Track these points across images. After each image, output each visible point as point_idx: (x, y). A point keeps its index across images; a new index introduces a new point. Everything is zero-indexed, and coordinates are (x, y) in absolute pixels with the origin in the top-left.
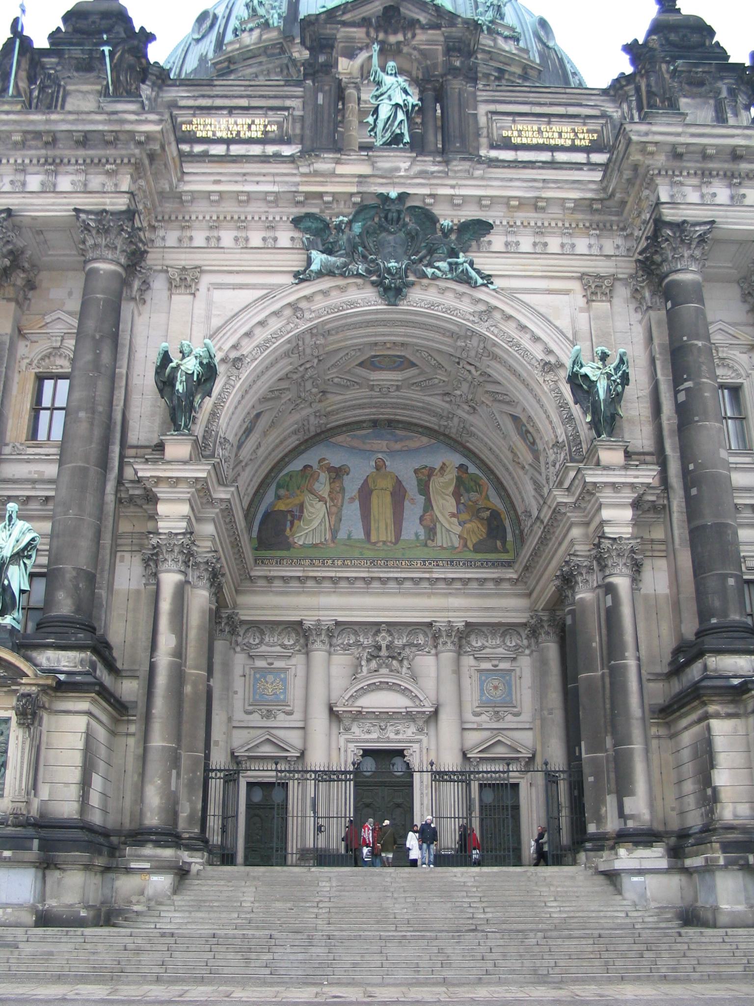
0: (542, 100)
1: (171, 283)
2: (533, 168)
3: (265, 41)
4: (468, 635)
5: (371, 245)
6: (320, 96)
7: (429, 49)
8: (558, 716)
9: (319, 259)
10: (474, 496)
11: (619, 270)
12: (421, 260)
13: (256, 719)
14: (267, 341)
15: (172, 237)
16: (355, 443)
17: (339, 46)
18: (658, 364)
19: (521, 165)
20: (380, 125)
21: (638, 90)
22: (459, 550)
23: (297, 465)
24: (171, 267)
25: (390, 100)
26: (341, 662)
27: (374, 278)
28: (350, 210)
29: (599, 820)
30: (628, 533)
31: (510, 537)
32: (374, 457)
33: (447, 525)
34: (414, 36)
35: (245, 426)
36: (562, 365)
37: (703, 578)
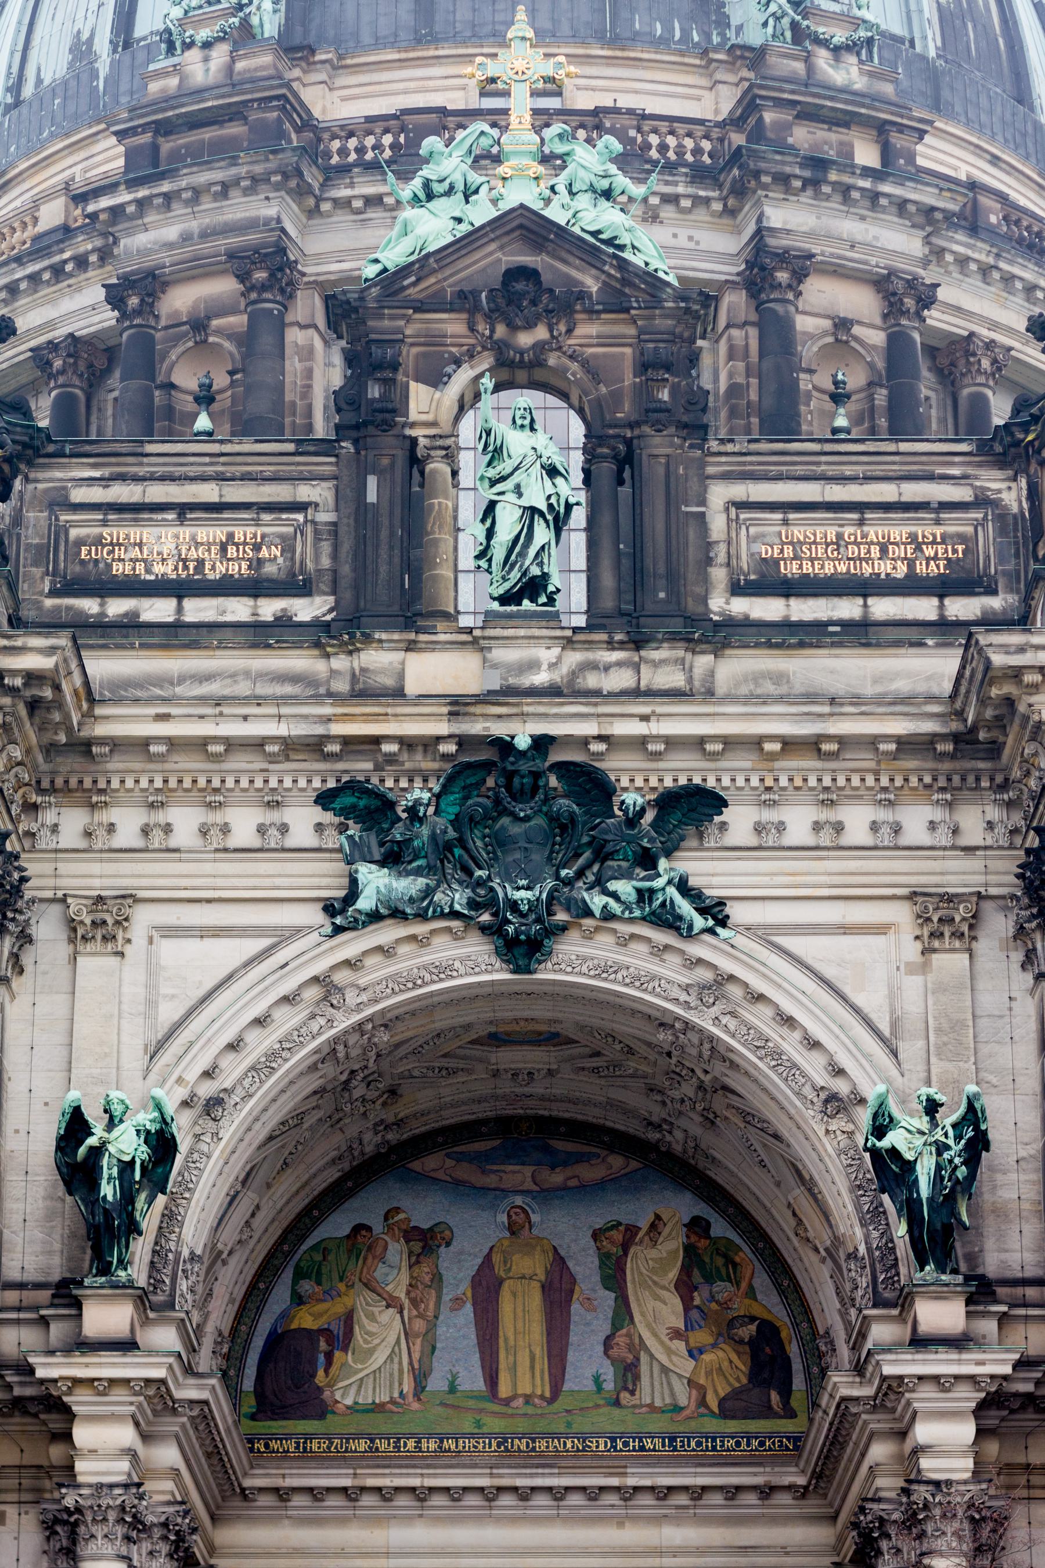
0: (848, 471)
1: (75, 930)
5: (479, 843)
6: (372, 482)
7: (605, 355)
10: (723, 1289)
11: (993, 879)
12: (580, 874)
14: (272, 1056)
16: (465, 1172)
17: (410, 354)
20: (498, 553)
22: (687, 1412)
25: (520, 495)
27: (486, 917)
28: (435, 765)
30: (966, 1470)
31: (798, 1382)
32: (505, 1204)
33: (663, 1358)
34: (570, 331)
36: (862, 1101)
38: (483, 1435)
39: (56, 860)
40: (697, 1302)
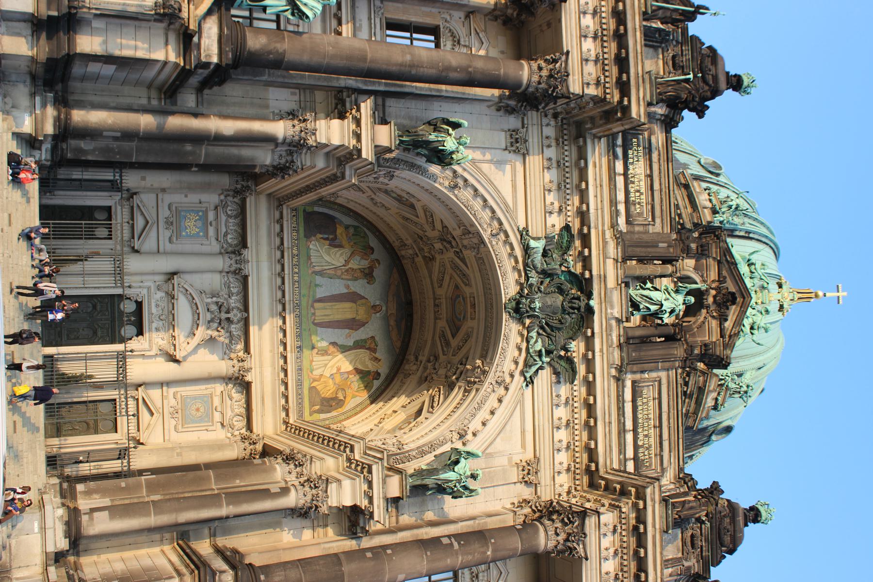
0: (671, 421)
2: (618, 415)
3: (703, 211)
4: (240, 385)
6: (665, 245)
8: (176, 461)
9: (538, 245)
11: (543, 488)
13: (164, 213)
15: (550, 131)
18: (471, 522)
19: (621, 405)
20: (646, 293)
21: (686, 494)
23: (373, 242)
24: (527, 131)
26: (215, 281)
29: (88, 493)
30: (332, 503)
32: (382, 304)
34: (713, 317)
35: (404, 195)
37: (298, 567)
38: (300, 298)
39: (538, 125)
40: (350, 376)
